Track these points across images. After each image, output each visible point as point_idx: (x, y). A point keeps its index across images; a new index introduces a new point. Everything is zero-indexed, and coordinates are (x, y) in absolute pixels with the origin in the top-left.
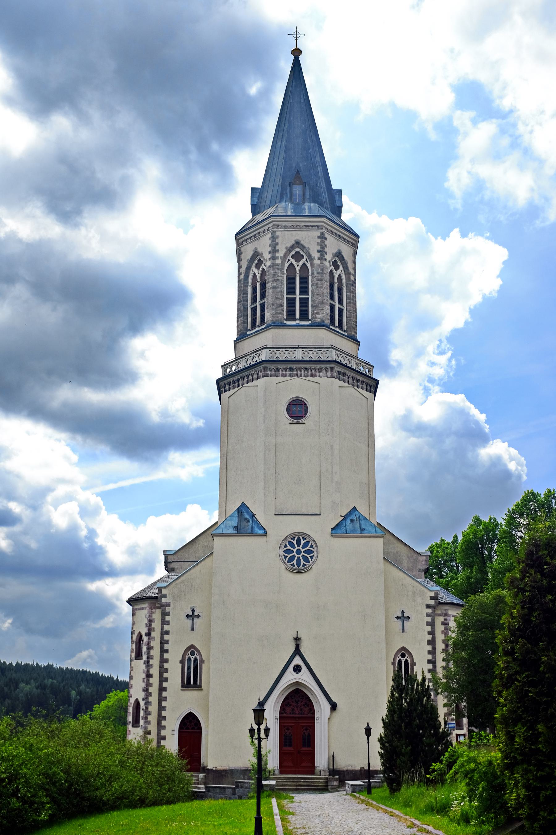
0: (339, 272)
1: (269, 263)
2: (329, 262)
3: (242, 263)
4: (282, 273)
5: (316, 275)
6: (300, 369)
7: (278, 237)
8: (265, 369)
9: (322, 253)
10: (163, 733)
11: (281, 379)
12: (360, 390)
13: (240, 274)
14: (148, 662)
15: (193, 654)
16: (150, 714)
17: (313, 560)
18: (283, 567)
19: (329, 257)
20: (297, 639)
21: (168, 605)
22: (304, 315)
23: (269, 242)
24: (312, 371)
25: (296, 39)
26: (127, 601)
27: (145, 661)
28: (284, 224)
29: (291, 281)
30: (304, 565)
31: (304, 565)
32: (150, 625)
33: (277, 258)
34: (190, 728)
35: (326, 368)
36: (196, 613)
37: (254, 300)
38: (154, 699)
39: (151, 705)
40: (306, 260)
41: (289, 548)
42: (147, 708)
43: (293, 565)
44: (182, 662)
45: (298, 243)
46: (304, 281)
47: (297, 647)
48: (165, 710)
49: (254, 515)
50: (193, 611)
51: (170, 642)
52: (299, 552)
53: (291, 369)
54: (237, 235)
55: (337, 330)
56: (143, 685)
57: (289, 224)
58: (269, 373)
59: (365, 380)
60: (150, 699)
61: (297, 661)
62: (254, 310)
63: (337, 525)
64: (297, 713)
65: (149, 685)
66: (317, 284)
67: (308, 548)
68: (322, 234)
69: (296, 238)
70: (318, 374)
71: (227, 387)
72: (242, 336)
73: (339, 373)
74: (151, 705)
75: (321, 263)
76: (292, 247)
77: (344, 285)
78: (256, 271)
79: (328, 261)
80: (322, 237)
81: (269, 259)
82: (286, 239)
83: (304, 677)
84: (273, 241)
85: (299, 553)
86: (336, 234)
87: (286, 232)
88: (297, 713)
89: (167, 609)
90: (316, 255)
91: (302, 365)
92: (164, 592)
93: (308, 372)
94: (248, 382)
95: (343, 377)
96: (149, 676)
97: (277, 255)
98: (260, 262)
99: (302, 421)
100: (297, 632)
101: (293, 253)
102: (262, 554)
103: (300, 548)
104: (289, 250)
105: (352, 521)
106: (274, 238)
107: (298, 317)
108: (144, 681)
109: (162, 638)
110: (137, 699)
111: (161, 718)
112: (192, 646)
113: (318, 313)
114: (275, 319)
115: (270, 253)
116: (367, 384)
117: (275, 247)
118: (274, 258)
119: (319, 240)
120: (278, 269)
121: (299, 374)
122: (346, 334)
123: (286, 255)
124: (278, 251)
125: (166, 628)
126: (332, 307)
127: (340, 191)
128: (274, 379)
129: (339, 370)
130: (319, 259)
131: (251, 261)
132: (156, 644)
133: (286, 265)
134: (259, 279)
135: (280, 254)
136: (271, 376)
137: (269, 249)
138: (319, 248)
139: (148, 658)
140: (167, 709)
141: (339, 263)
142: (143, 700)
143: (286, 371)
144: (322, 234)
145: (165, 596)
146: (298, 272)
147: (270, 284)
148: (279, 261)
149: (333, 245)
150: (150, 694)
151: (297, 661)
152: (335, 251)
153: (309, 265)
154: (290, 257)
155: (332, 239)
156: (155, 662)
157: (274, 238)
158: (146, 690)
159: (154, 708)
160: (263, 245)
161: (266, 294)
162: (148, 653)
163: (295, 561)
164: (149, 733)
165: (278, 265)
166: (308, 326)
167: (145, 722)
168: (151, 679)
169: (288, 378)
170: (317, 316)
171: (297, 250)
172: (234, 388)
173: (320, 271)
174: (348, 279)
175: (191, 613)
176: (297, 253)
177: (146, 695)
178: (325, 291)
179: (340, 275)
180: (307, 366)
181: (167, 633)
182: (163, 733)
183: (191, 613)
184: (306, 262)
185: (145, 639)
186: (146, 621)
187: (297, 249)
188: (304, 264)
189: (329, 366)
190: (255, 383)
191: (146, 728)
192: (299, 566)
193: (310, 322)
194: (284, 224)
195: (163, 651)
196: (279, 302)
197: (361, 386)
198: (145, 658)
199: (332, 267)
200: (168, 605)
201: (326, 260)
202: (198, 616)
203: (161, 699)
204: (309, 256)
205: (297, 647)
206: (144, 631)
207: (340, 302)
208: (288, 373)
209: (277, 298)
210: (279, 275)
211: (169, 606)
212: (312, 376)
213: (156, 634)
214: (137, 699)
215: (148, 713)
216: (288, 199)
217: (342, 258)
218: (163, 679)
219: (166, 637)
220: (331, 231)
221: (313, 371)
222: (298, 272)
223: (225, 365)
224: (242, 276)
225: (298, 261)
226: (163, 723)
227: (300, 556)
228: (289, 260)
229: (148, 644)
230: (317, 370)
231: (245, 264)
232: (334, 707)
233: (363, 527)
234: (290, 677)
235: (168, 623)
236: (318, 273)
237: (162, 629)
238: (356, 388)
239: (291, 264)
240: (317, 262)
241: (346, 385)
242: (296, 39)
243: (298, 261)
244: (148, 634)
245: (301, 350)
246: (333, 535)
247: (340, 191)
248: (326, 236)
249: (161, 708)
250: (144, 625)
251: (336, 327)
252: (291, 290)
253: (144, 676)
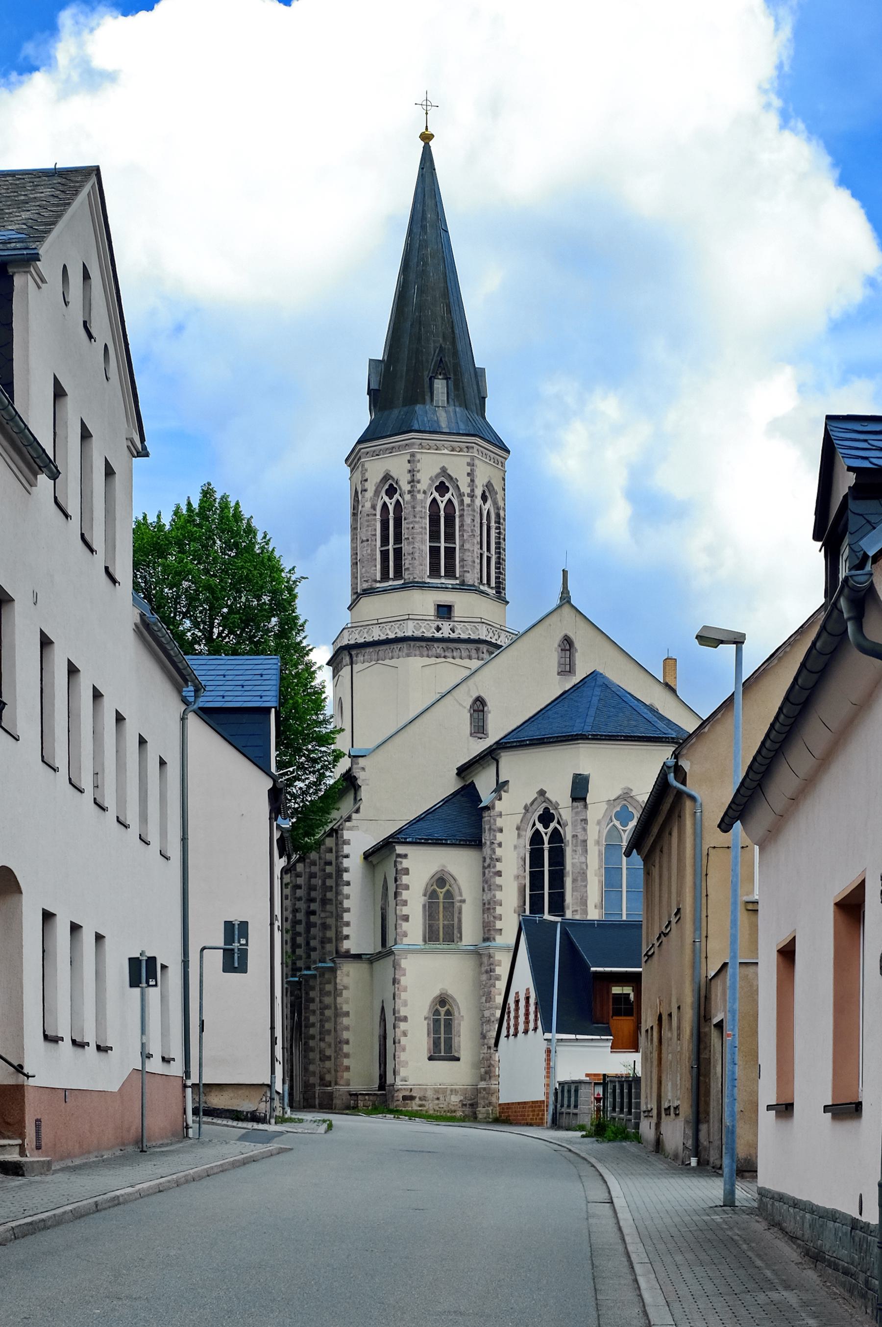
0: (448, 496)
9: (412, 482)
68: (413, 455)
77: (457, 513)
82: (375, 469)
90: (406, 487)
101: (387, 487)
123: (377, 493)
135: (370, 494)
154: (383, 493)
176: (391, 485)
179: (450, 500)
188: (398, 501)
217: (450, 478)
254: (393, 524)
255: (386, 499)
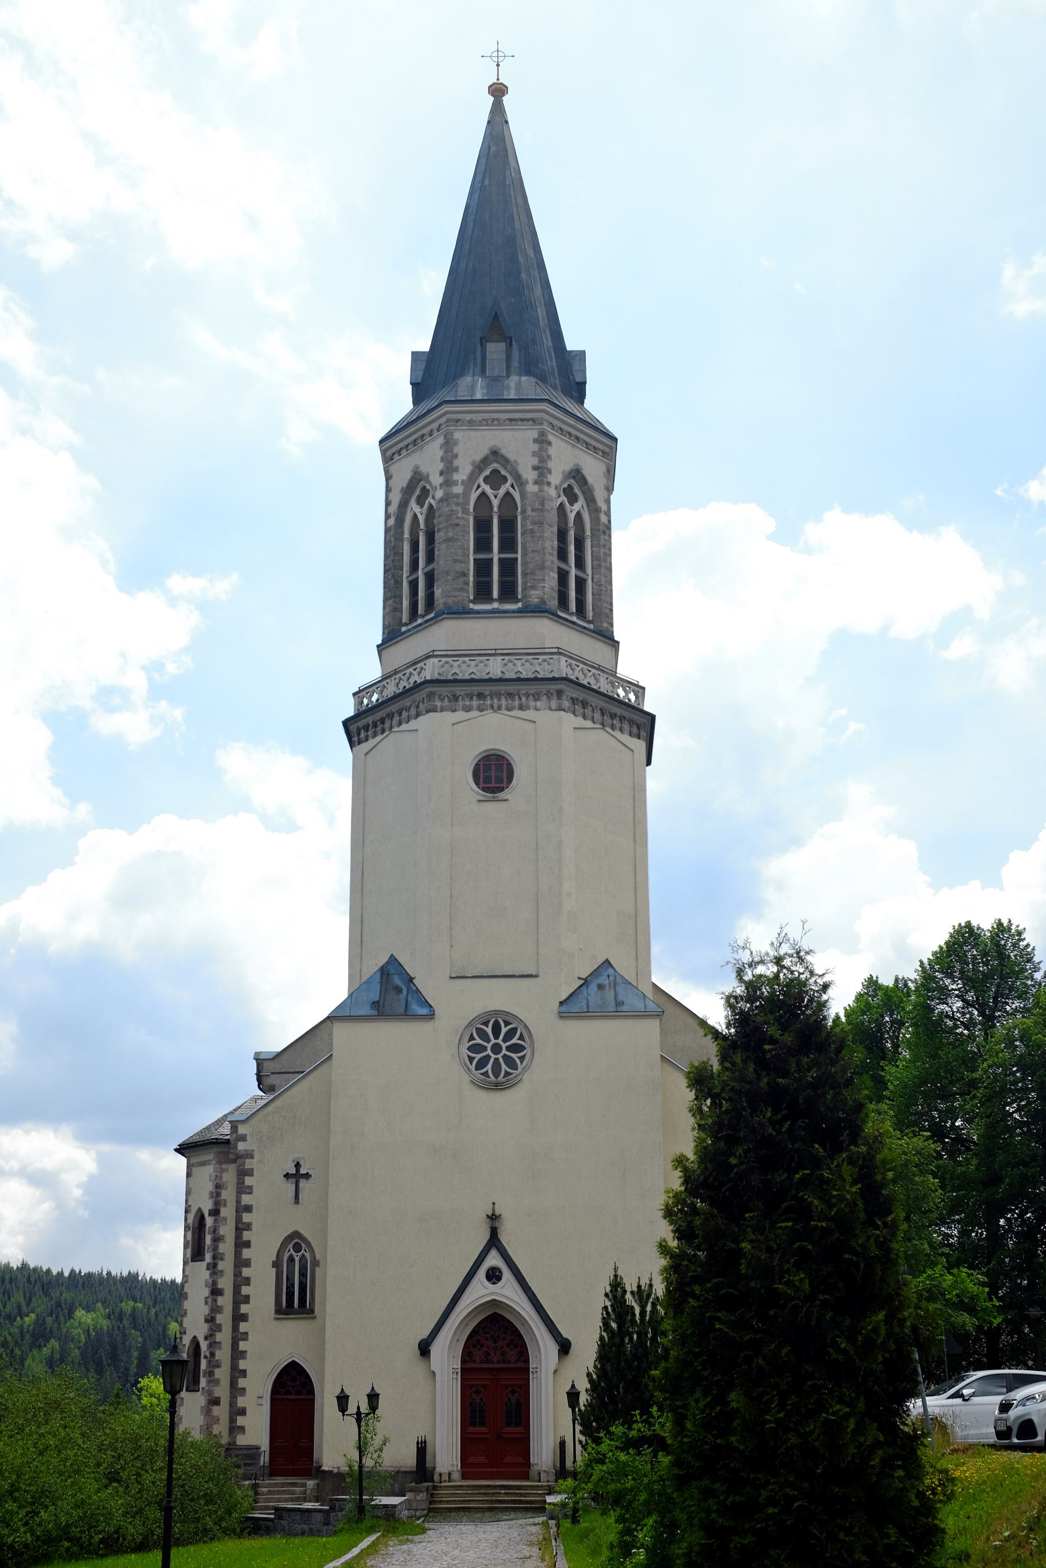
0: (577, 507)
1: (439, 494)
2: (556, 488)
3: (391, 496)
4: (466, 511)
5: (529, 513)
6: (499, 695)
7: (456, 443)
8: (431, 696)
10: (241, 1402)
11: (460, 715)
12: (617, 733)
13: (387, 516)
14: (215, 1265)
15: (297, 1248)
16: (218, 1366)
17: (525, 1063)
18: (466, 1078)
19: (555, 478)
20: (493, 1218)
21: (250, 1155)
22: (508, 592)
23: (441, 453)
24: (520, 699)
25: (498, 65)
26: (176, 1150)
27: (208, 1264)
28: (468, 417)
29: (483, 527)
30: (507, 1074)
31: (507, 1074)
32: (218, 1194)
33: (455, 483)
34: (294, 1388)
35: (548, 692)
36: (303, 1171)
37: (414, 566)
38: (224, 1337)
39: (220, 1348)
40: (512, 486)
41: (478, 1041)
42: (213, 1354)
43: (486, 1074)
44: (277, 1264)
45: (495, 453)
46: (508, 526)
47: (494, 1233)
48: (245, 1358)
49: (411, 980)
50: (298, 1166)
51: (254, 1227)
52: (496, 1049)
53: (481, 696)
54: (381, 442)
55: (574, 619)
56: (206, 1310)
57: (478, 417)
58: (438, 704)
59: (626, 714)
60: (219, 1337)
61: (494, 1260)
62: (414, 585)
63: (571, 995)
64: (495, 1360)
65: (215, 1309)
66: (532, 531)
67: (515, 1041)
68: (542, 434)
69: (491, 444)
70: (532, 703)
71: (362, 735)
72: (392, 636)
73: (574, 701)
74: (220, 1348)
75: (541, 490)
76: (485, 462)
77: (588, 533)
78: (417, 509)
79: (553, 485)
80: (542, 441)
81: (441, 485)
82: (472, 446)
83: (508, 1291)
84: (446, 452)
85: (497, 1050)
86: (570, 434)
87: (473, 434)
88: (495, 1360)
89: (249, 1164)
90: (529, 475)
91: (502, 688)
92: (242, 1130)
93: (513, 700)
94: (400, 724)
95: (581, 710)
96: (216, 1292)
97: (456, 477)
98: (425, 493)
99: (501, 795)
100: (494, 1204)
101: (487, 472)
102: (426, 1054)
103: (500, 1041)
104: (479, 467)
105: (600, 987)
106: (449, 445)
107: (495, 594)
108: (206, 1303)
109: (238, 1219)
110: (195, 1337)
111: (237, 1373)
112: (296, 1234)
113: (533, 588)
114: (450, 601)
115: (441, 473)
116: (631, 722)
117: (451, 462)
118: (448, 483)
119: (536, 447)
120: (458, 504)
121: (495, 706)
122: (591, 626)
123: (472, 478)
124: (456, 470)
125: (246, 1199)
126: (563, 576)
127: (582, 354)
128: (449, 717)
129: (575, 696)
130: (536, 483)
131: (408, 491)
132: (227, 1231)
133: (474, 496)
134: (422, 526)
135: (461, 476)
136: (442, 711)
137: (441, 466)
138: (535, 461)
139: (214, 1257)
140: (248, 1355)
141: (577, 491)
142: (206, 1338)
143: (471, 699)
144: (542, 434)
145: (243, 1138)
146: (495, 509)
147: (441, 534)
148: (458, 489)
149: (563, 456)
150: (219, 1328)
151: (494, 1260)
152: (568, 467)
153: (517, 495)
154: (481, 480)
155: (563, 444)
156: (226, 1265)
157: (449, 445)
158: (210, 1320)
159: (223, 1355)
160: (429, 459)
161: (436, 553)
162: (215, 1249)
163: (489, 1067)
164: (216, 1402)
165: (457, 496)
166: (514, 612)
167: (209, 1382)
168: (219, 1298)
169: (475, 713)
170: (532, 592)
171: (495, 467)
172: (375, 735)
173: (537, 506)
174: (596, 520)
175: (293, 1171)
176: (495, 472)
177: (211, 1329)
178: (548, 544)
179: (578, 514)
180: (512, 688)
181: (248, 1209)
182: (241, 1402)
183: (293, 1171)
184: (511, 490)
185: (209, 1221)
186: (210, 1187)
187: (495, 465)
188: (508, 493)
189: (553, 687)
190: (413, 724)
191: (210, 1393)
192: (496, 1076)
193: (520, 605)
194: (468, 417)
195: (241, 1244)
196: (459, 567)
197: (618, 725)
198: (208, 1257)
199: (563, 499)
200: (250, 1155)
201: (549, 484)
202: (307, 1176)
203: (238, 1337)
204: (518, 477)
205: (494, 1233)
206: (207, 1206)
207: (580, 564)
208: (475, 703)
209: (456, 561)
210: (460, 515)
211: (252, 1157)
212: (521, 708)
213: (228, 1212)
214: (195, 1337)
215: (214, 1364)
216: (478, 370)
217: (582, 481)
218: (240, 1299)
219: (246, 1218)
220: (561, 429)
221: (524, 699)
222: (495, 509)
223: (360, 691)
224: (392, 522)
225: (495, 487)
226: (242, 1383)
227: (500, 1056)
228: (479, 487)
229: (215, 1230)
230: (531, 697)
231: (396, 498)
232: (564, 1347)
233: (621, 998)
234: (481, 1291)
235: (249, 1190)
236: (533, 510)
237: (238, 1202)
238: (609, 730)
239: (483, 494)
240: (532, 488)
241: (589, 724)
242: (498, 65)
243: (495, 487)
244: (215, 1212)
245: (499, 658)
246: (562, 1016)
247: (582, 354)
248: (551, 438)
249: (237, 1355)
250: (208, 1195)
251: (571, 614)
252: (483, 544)
253: (206, 1292)
254: (498, 527)
255: (487, 489)
